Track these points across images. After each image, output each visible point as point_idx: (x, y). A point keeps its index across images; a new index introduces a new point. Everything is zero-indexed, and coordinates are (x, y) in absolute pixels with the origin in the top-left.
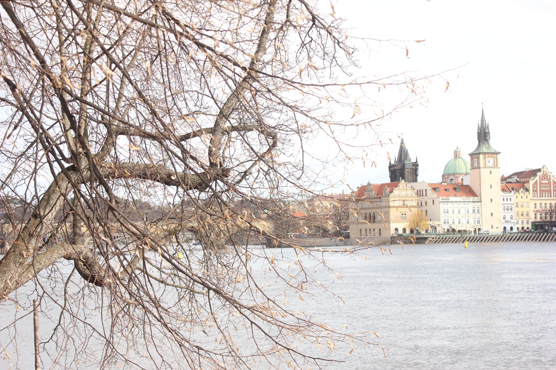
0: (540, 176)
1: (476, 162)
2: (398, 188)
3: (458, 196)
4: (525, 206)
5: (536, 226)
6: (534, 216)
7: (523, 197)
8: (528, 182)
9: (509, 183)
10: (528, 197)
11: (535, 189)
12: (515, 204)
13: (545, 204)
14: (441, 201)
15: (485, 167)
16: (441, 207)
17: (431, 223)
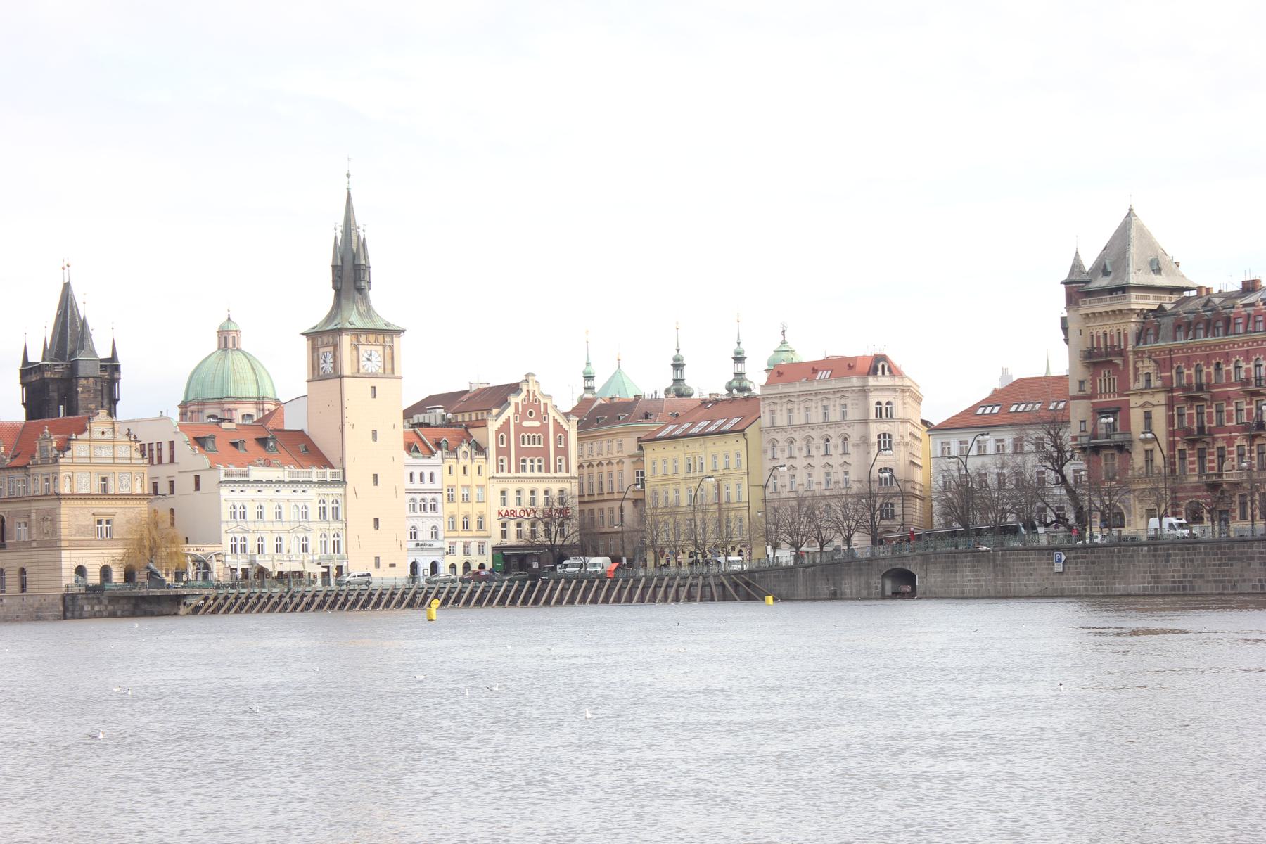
0: (517, 404)
1: (330, 359)
2: (86, 435)
3: (275, 466)
4: (473, 498)
5: (506, 559)
6: (499, 529)
7: (468, 470)
8: (483, 424)
9: (421, 425)
10: (482, 470)
11: (504, 446)
12: (445, 493)
13: (532, 492)
14: (223, 479)
15: (357, 374)
16: (222, 499)
17: (192, 548)
